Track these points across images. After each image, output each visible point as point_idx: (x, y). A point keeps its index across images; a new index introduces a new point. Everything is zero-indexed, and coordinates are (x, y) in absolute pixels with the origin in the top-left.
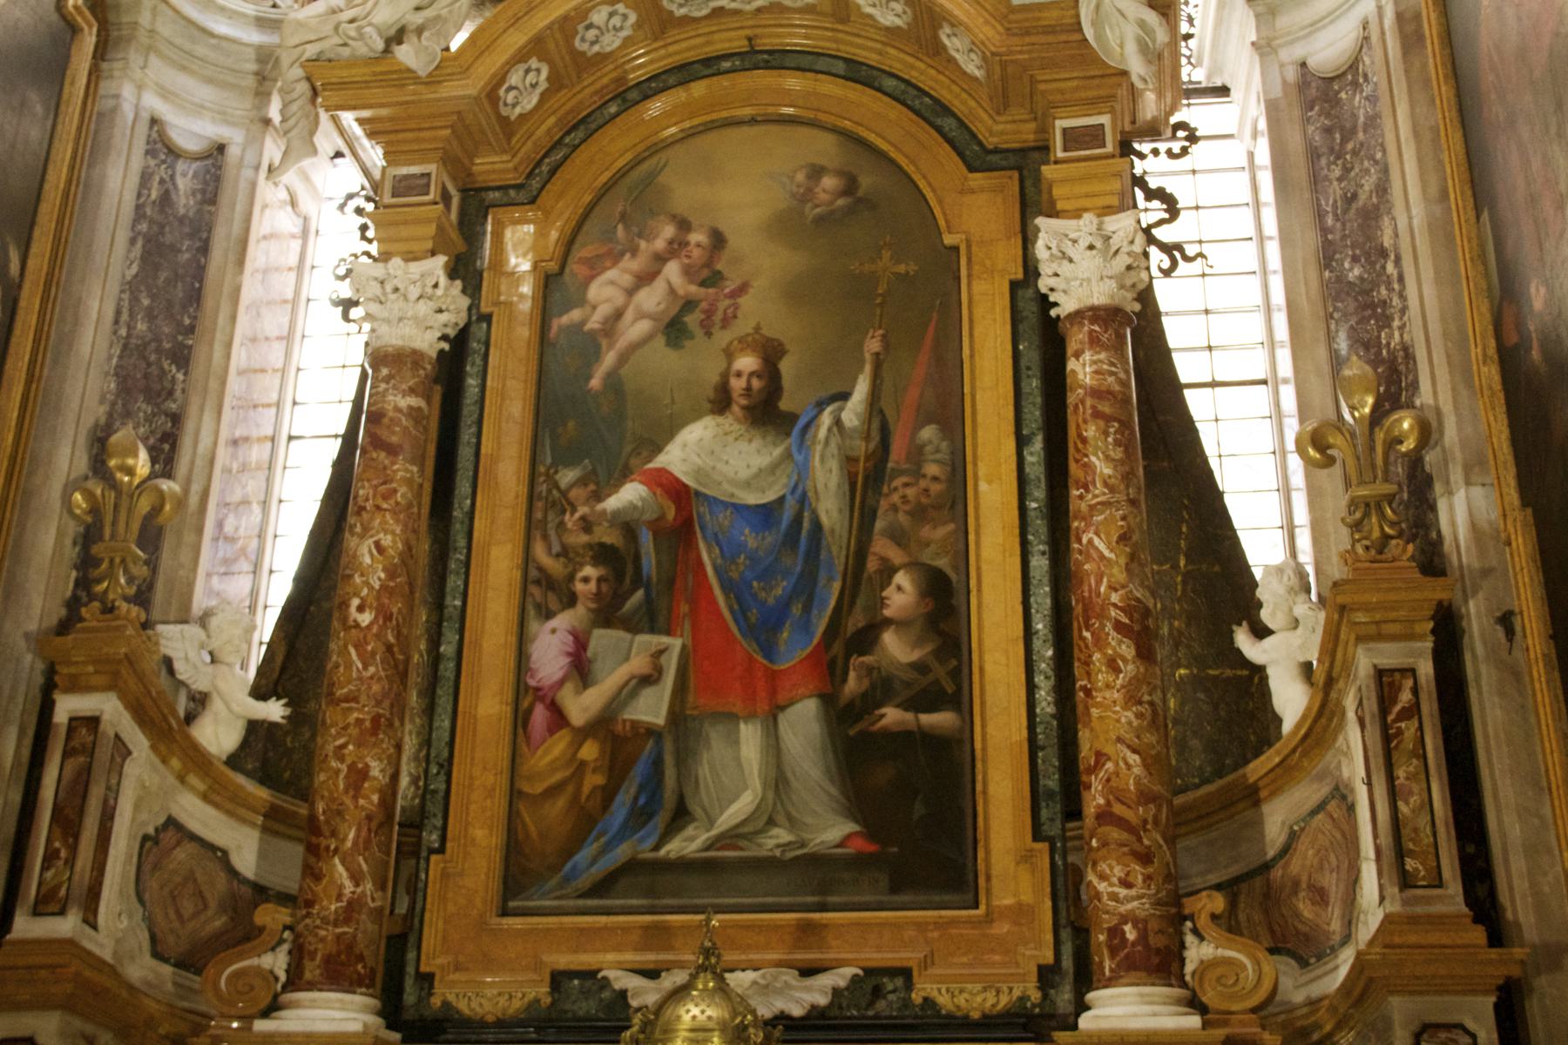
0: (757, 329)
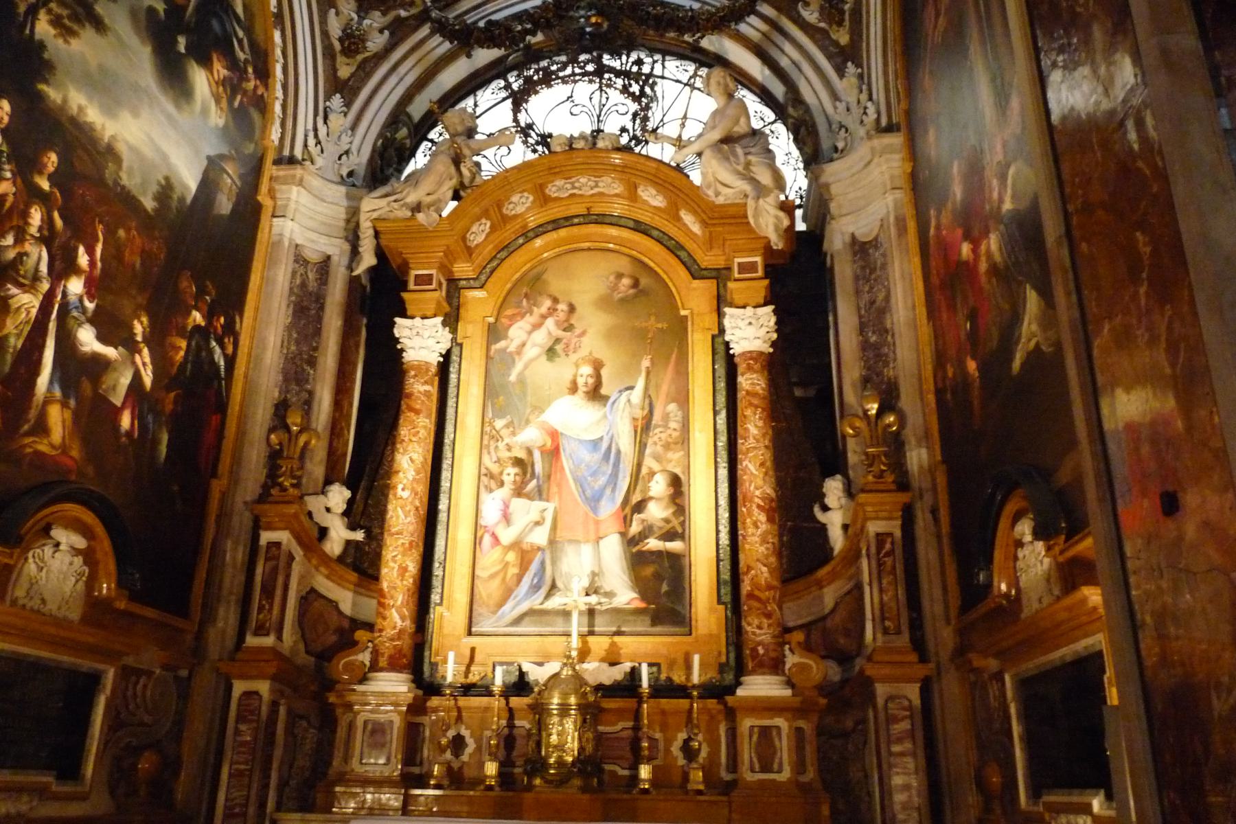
0: (591, 353)
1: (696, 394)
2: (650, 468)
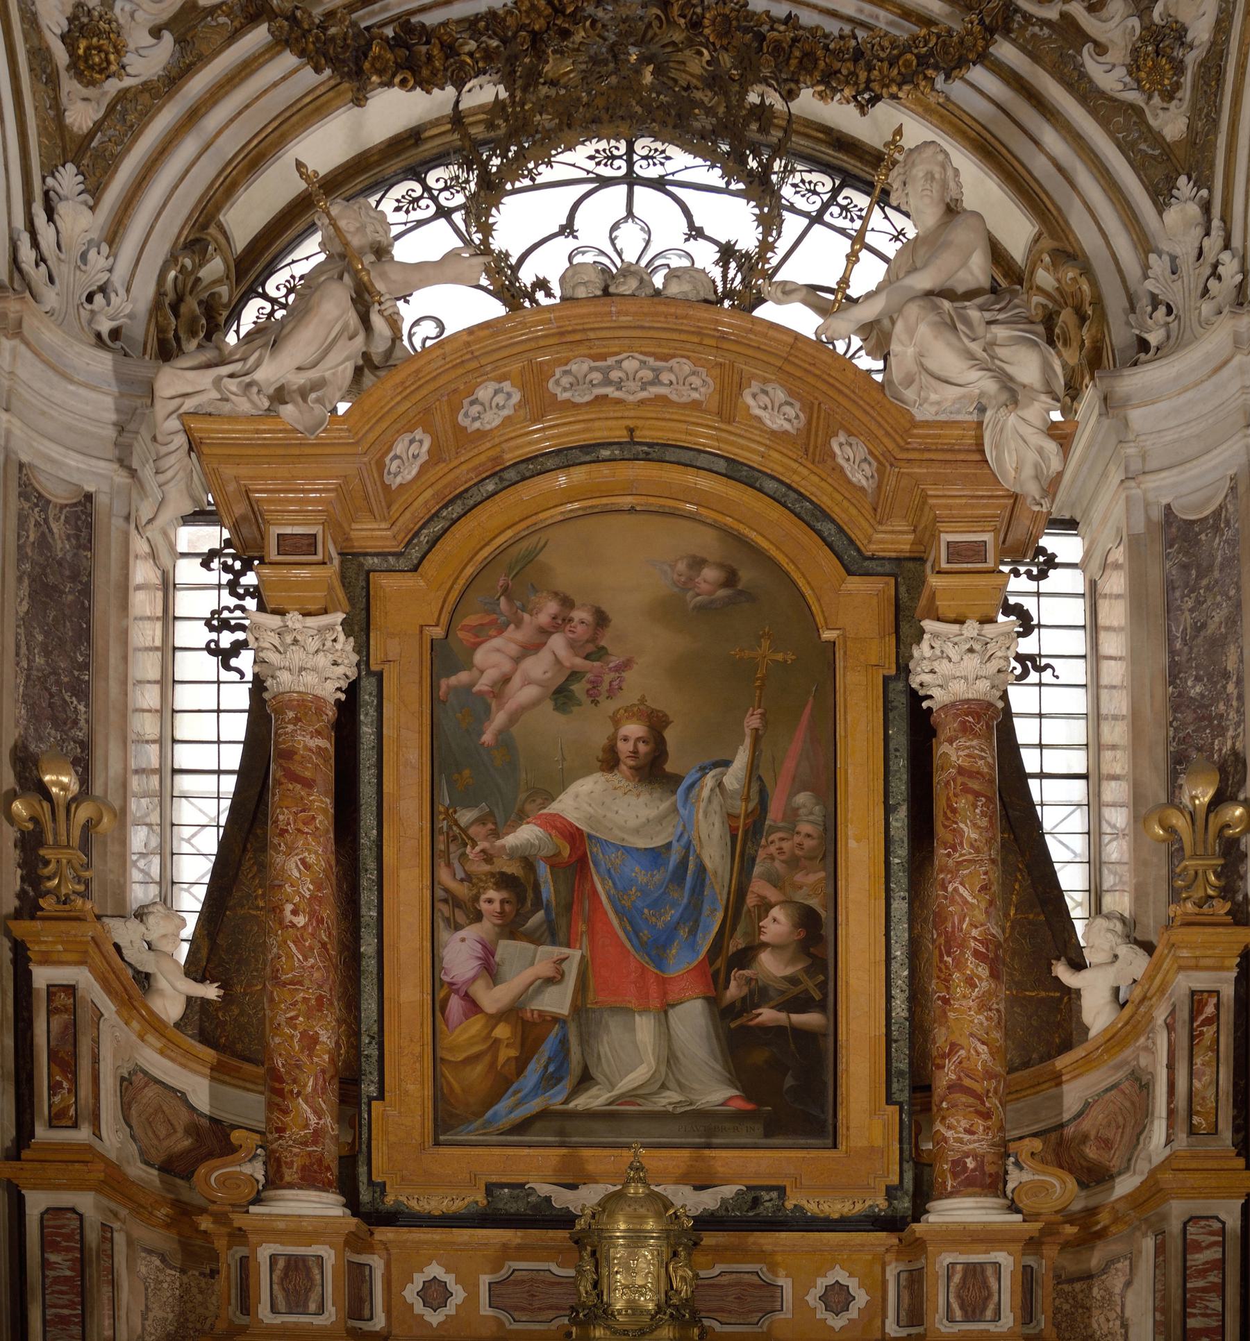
0: (642, 700)
1: (851, 778)
2: (762, 898)
